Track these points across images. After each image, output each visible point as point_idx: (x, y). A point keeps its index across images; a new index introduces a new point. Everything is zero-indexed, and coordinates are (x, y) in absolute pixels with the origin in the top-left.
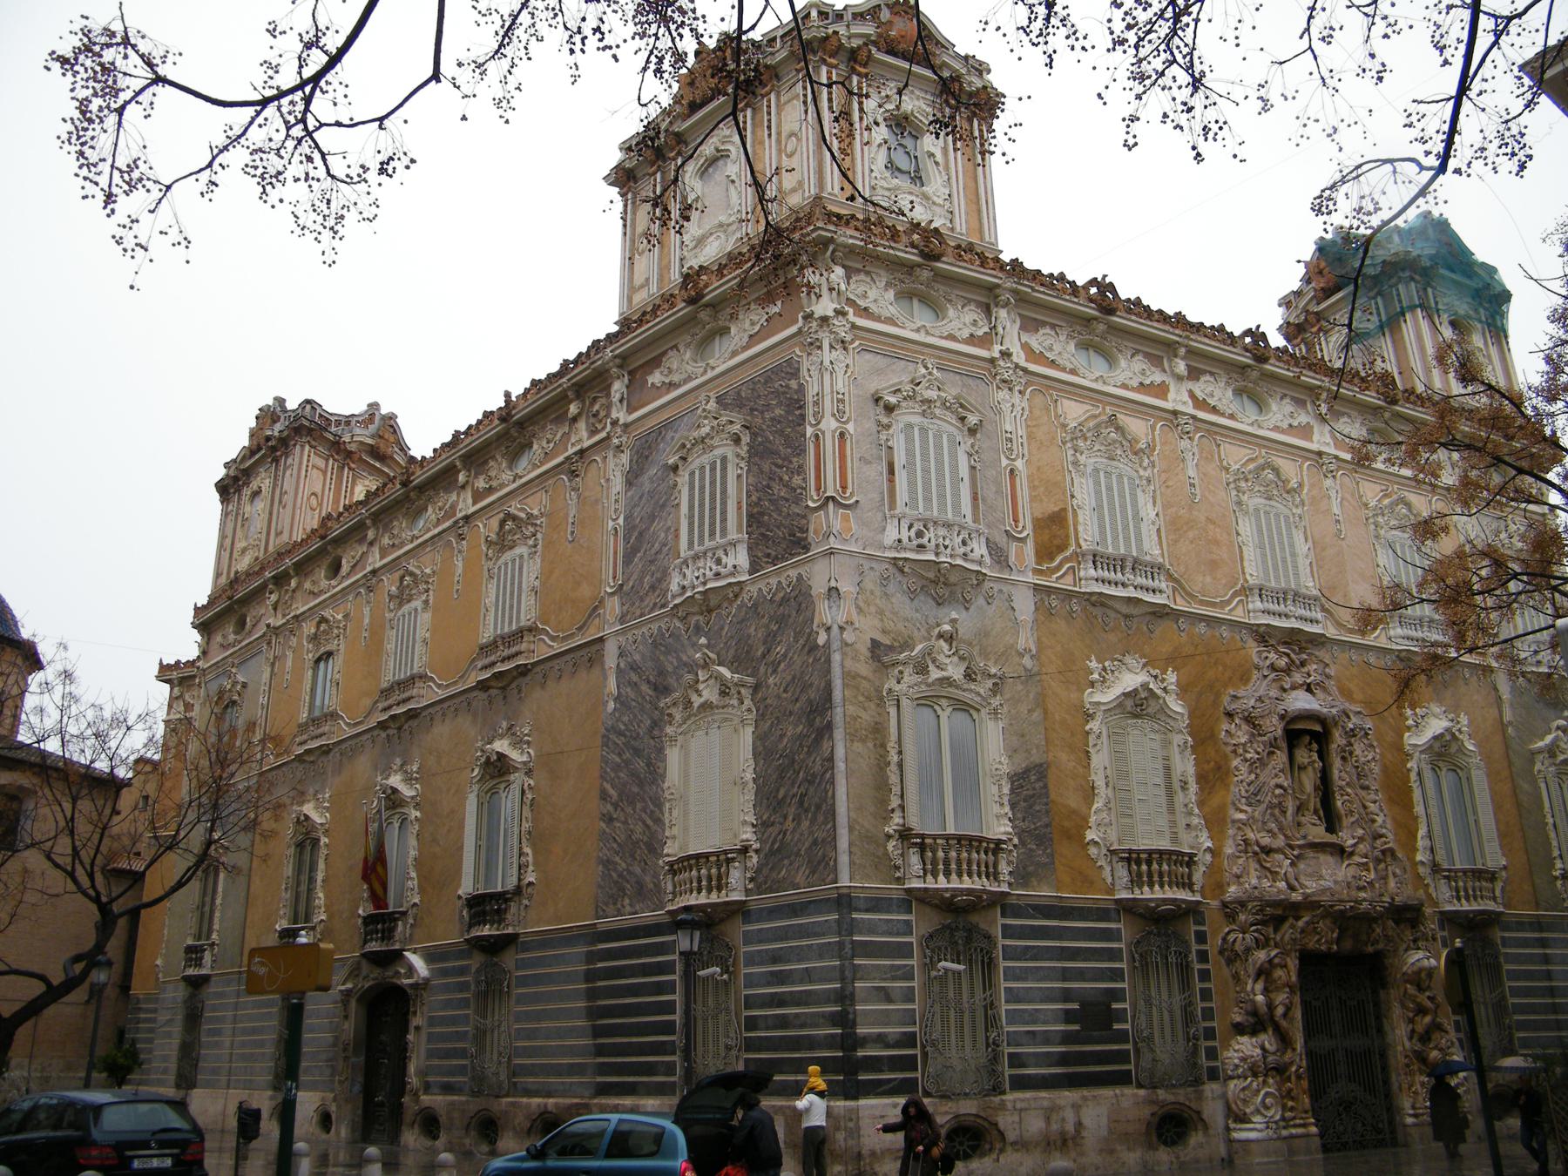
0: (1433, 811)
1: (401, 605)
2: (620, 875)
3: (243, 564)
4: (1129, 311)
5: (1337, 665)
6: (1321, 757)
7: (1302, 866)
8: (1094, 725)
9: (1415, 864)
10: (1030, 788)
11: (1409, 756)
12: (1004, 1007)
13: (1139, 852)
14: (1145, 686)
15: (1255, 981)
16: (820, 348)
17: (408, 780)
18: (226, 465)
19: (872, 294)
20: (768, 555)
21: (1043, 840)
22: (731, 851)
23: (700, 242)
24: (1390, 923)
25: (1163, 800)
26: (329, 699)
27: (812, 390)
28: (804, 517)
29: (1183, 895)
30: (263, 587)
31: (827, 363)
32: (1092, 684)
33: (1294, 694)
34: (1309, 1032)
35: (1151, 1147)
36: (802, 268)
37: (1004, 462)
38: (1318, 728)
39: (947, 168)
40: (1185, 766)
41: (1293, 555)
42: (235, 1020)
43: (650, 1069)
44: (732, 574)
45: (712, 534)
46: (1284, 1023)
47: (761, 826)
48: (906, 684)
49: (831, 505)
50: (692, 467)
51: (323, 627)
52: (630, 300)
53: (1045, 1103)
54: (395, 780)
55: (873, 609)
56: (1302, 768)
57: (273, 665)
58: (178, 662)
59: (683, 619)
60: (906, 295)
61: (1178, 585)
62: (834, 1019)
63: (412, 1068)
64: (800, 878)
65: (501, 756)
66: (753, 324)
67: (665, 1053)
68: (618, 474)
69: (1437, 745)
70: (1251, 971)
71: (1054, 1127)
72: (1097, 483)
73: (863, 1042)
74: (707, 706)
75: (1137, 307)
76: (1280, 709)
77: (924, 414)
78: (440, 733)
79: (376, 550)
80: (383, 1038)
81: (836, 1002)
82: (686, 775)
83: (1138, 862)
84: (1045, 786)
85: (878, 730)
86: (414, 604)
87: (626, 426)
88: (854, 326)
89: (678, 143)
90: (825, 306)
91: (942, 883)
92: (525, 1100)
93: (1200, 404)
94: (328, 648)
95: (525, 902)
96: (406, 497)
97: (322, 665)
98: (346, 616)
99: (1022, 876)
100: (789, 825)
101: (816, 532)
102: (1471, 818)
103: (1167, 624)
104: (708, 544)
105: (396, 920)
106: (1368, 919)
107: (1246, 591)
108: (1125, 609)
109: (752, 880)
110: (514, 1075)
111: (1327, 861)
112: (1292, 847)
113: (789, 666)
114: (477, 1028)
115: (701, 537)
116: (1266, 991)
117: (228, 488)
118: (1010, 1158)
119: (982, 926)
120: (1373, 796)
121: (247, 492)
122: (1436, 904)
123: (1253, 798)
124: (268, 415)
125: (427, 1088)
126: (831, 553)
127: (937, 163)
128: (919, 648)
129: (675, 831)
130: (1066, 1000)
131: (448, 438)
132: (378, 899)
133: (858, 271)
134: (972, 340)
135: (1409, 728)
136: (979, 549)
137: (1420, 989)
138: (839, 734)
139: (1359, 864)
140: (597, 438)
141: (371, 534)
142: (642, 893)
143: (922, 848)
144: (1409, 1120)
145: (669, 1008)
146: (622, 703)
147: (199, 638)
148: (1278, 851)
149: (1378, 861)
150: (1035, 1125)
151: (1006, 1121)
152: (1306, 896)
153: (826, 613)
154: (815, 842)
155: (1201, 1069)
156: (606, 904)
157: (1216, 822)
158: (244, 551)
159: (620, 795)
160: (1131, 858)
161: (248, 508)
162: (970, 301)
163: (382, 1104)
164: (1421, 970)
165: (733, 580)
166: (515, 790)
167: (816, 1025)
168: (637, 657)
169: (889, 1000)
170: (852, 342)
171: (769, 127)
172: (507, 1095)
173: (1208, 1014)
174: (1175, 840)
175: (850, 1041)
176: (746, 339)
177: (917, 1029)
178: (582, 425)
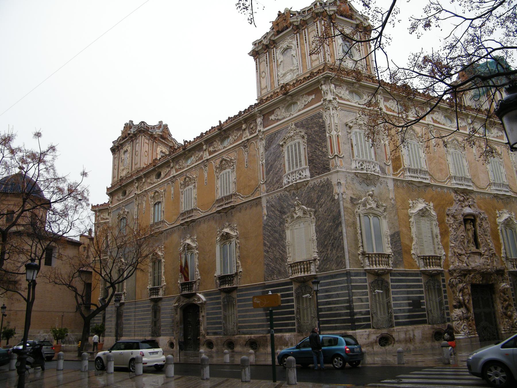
0: (506, 242)
1: (185, 187)
2: (272, 268)
3: (123, 174)
5: (477, 198)
6: (474, 227)
7: (470, 259)
8: (412, 220)
9: (501, 257)
10: (396, 239)
12: (392, 302)
13: (426, 256)
14: (425, 207)
16: (329, 109)
17: (193, 241)
18: (113, 142)
19: (342, 92)
20: (316, 172)
21: (400, 254)
22: (311, 260)
23: (284, 75)
24: (496, 275)
25: (431, 241)
26: (160, 217)
27: (327, 122)
28: (328, 161)
29: (439, 268)
30: (132, 182)
31: (332, 114)
32: (410, 208)
33: (466, 208)
34: (474, 308)
35: (433, 341)
36: (322, 85)
38: (473, 218)
40: (437, 231)
41: (463, 166)
42: (135, 316)
43: (287, 325)
44: (305, 178)
45: (297, 165)
46: (468, 305)
47: (320, 253)
48: (361, 210)
49: (336, 157)
50: (288, 145)
51: (157, 194)
52: (261, 92)
53: (405, 330)
54: (188, 241)
55: (350, 188)
56: (468, 230)
57: (138, 206)
58: (98, 205)
59: (288, 192)
60: (351, 92)
61: (432, 177)
62: (347, 308)
63: (202, 328)
64: (333, 267)
65: (227, 233)
66: (305, 101)
67: (291, 320)
68: (262, 147)
69: (506, 222)
70: (458, 290)
71: (408, 336)
73: (356, 314)
74: (299, 217)
76: (462, 213)
77: (359, 128)
78: (204, 227)
79: (174, 170)
80: (189, 319)
81: (347, 303)
82: (293, 238)
83: (426, 260)
84: (400, 238)
85: (354, 223)
86: (190, 187)
87: (263, 132)
88: (338, 103)
89: (274, 43)
90: (330, 97)
91: (375, 267)
92: (243, 336)
93: (435, 121)
94: (159, 200)
95: (239, 277)
96: (184, 153)
97: (157, 206)
98: (165, 191)
99: (395, 265)
100: (329, 252)
101: (332, 165)
103: (429, 189)
104: (295, 169)
105: (193, 284)
106: (490, 274)
107: (450, 178)
108: (417, 184)
109: (318, 268)
110: (239, 329)
111: (477, 257)
112: (467, 253)
113: (326, 205)
114: (224, 315)
115: (293, 166)
116: (462, 296)
117: (115, 149)
118: (396, 345)
120: (488, 238)
121: (122, 151)
122: (507, 269)
123: (455, 240)
124: (129, 126)
125: (208, 334)
126: (338, 172)
128: (364, 199)
129: (290, 255)
130: (409, 300)
131: (199, 135)
132: (186, 278)
133: (338, 85)
135: (498, 217)
136: (378, 169)
137: (505, 294)
138: (343, 225)
139: (486, 258)
140: (253, 136)
141: (172, 165)
142: (280, 273)
143: (369, 257)
144: (503, 332)
145: (292, 306)
146: (269, 217)
147: (109, 197)
148: (464, 255)
149: (491, 257)
150: (402, 336)
151: (395, 335)
152: (473, 268)
153: (337, 190)
154: (338, 257)
155: (445, 318)
156: (268, 277)
157: (446, 247)
158: (123, 170)
159: (270, 244)
160: (424, 258)
161: (123, 156)
163: (190, 339)
164: (505, 288)
166: (233, 243)
167: (341, 310)
168: (273, 203)
169: (362, 302)
171: (306, 40)
172: (237, 335)
173: (446, 303)
174: (435, 252)
175: (352, 314)
177: (370, 310)
178: (247, 131)
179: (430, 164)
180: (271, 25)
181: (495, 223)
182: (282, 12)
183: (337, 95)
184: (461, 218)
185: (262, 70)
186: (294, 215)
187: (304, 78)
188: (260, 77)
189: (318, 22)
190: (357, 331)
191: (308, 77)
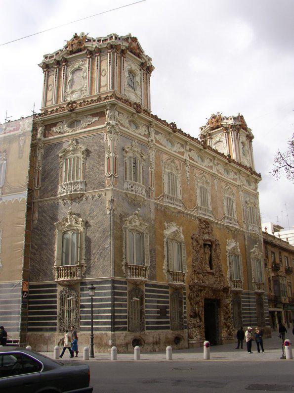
4: (179, 132)
7: (205, 277)
12: (145, 309)
13: (174, 272)
19: (124, 120)
20: (92, 187)
36: (107, 110)
37: (150, 169)
39: (141, 87)
45: (73, 178)
66: (90, 121)
68: (40, 154)
72: (169, 177)
75: (180, 130)
87: (44, 141)
91: (134, 278)
93: (191, 158)
100: (96, 260)
106: (219, 291)
133: (120, 113)
136: (144, 193)
137: (227, 308)
143: (130, 268)
150: (151, 340)
160: (173, 274)
162: (144, 125)
179: (183, 194)
180: (65, 44)
182: (78, 35)
183: (119, 122)
184: (201, 242)
185: (49, 83)
187: (92, 100)
188: (47, 89)
189: (111, 53)
190: (116, 333)
191: (95, 101)
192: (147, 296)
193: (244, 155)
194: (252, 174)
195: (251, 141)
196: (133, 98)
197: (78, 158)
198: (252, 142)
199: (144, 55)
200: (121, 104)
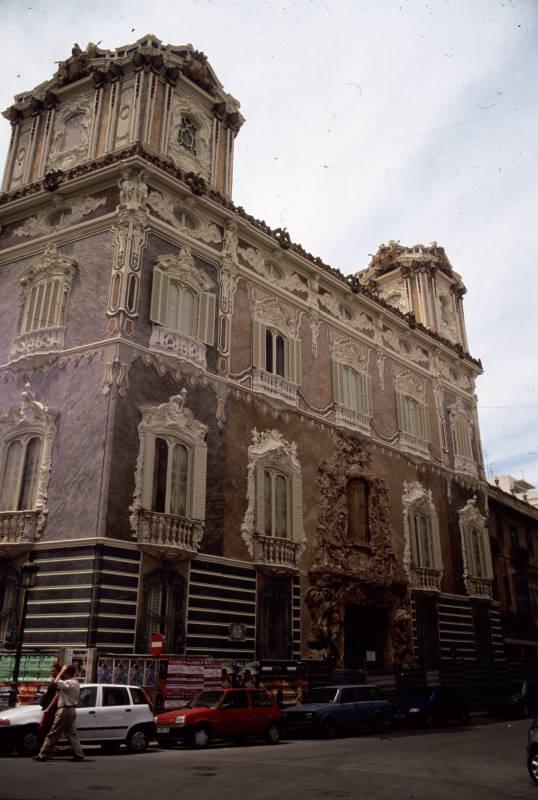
7: (350, 558)
11: (404, 507)
12: (188, 622)
14: (281, 448)
15: (323, 619)
16: (127, 226)
19: (161, 205)
24: (391, 594)
31: (130, 235)
36: (123, 181)
39: (211, 151)
44: (51, 348)
46: (336, 644)
49: (122, 314)
52: (9, 185)
75: (298, 249)
88: (149, 219)
91: (160, 544)
93: (323, 307)
102: (429, 543)
116: (328, 625)
119: (180, 572)
127: (205, 146)
133: (155, 190)
134: (211, 244)
135: (405, 493)
137: (402, 630)
148: (340, 548)
162: (213, 223)
164: (403, 620)
165: (53, 352)
170: (146, 228)
171: (113, 101)
176: (81, 216)
180: (56, 68)
181: (400, 500)
182: (84, 48)
183: (148, 205)
184: (343, 480)
186: (16, 418)
189: (142, 73)
192: (194, 590)
193: (446, 321)
194: (462, 357)
195: (459, 298)
196: (186, 164)
197: (57, 282)
198: (462, 299)
199: (224, 93)
200: (151, 167)
